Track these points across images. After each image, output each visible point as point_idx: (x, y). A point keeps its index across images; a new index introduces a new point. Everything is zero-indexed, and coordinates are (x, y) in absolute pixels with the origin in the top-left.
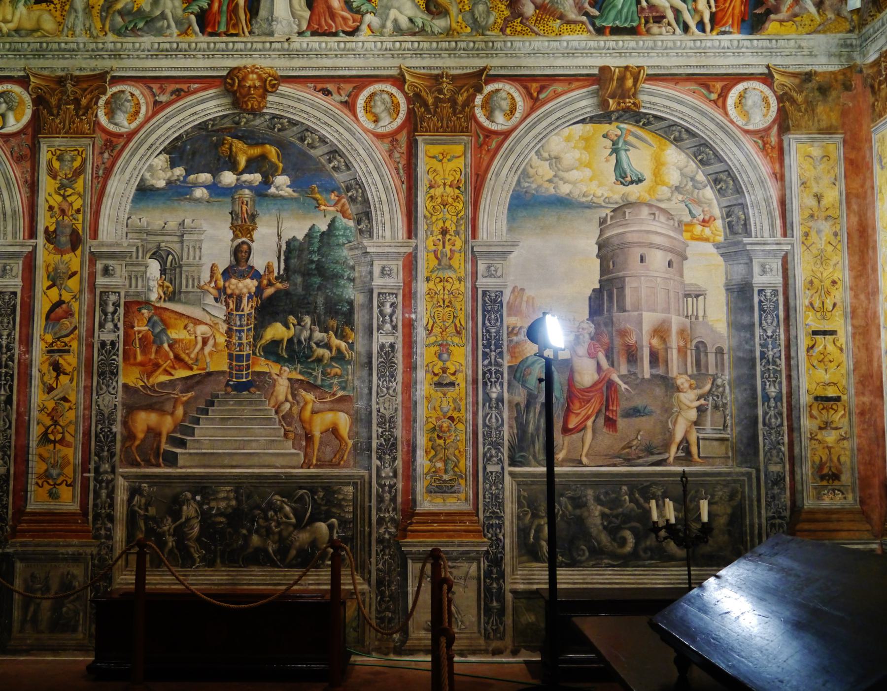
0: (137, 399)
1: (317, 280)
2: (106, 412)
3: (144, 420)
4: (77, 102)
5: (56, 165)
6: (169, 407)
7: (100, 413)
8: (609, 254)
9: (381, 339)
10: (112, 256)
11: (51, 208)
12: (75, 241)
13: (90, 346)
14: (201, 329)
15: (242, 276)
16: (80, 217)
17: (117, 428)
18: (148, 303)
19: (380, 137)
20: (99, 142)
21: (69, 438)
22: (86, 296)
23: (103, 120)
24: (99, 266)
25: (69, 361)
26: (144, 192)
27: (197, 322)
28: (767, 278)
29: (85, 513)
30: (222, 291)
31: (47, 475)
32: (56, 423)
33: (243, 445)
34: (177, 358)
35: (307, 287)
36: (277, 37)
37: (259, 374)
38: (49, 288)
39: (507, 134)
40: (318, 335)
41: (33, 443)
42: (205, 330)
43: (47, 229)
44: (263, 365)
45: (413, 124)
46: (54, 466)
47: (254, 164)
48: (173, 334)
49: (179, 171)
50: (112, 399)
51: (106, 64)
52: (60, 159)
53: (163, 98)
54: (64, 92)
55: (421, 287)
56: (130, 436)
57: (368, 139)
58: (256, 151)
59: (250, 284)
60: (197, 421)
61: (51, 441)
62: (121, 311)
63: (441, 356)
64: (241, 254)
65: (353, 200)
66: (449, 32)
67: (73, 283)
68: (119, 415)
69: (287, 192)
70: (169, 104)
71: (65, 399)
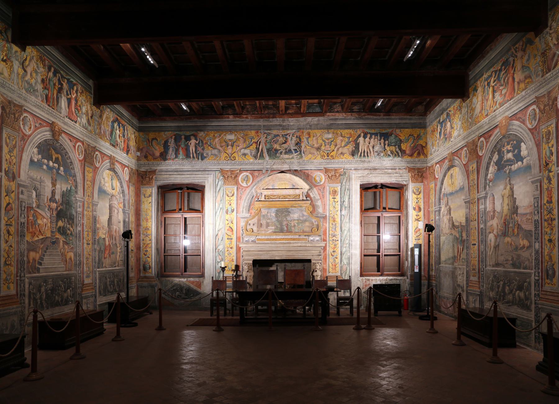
0: (32, 247)
1: (68, 207)
2: (22, 251)
3: (32, 255)
4: (14, 114)
5: (8, 140)
6: (38, 250)
7: (21, 252)
8: (111, 208)
9: (79, 229)
10: (24, 186)
11: (6, 160)
12: (14, 178)
13: (18, 224)
14: (45, 220)
15: (53, 202)
16: (15, 166)
17: (25, 259)
18: (33, 208)
19: (80, 161)
20: (21, 136)
21: (12, 263)
22: (17, 202)
23: (22, 126)
24: (21, 189)
25: (12, 229)
26: (32, 161)
27: (44, 218)
28: (127, 220)
29: (17, 295)
30: (49, 206)
31: (6, 280)
32: (9, 257)
33: (53, 265)
34: (40, 231)
35: (66, 208)
36: (62, 115)
37: (57, 238)
38: (6, 196)
39: (98, 168)
40: (68, 226)
41: (2, 266)
42: (45, 220)
43: (5, 169)
44: (58, 236)
45: (85, 158)
46: (8, 275)
47: (57, 161)
48: (39, 222)
49: (40, 156)
50: (24, 247)
51: (23, 103)
52: (9, 138)
53: (37, 125)
54: (11, 108)
55: (85, 213)
56: (29, 262)
57: (77, 160)
58: (57, 156)
59: (54, 205)
60: (44, 255)
61: (8, 265)
62: (26, 210)
63: (87, 236)
64: (53, 193)
65: (74, 180)
66: (91, 131)
67: (13, 195)
68: (26, 252)
69: (62, 173)
70: (39, 128)
71: (11, 246)
